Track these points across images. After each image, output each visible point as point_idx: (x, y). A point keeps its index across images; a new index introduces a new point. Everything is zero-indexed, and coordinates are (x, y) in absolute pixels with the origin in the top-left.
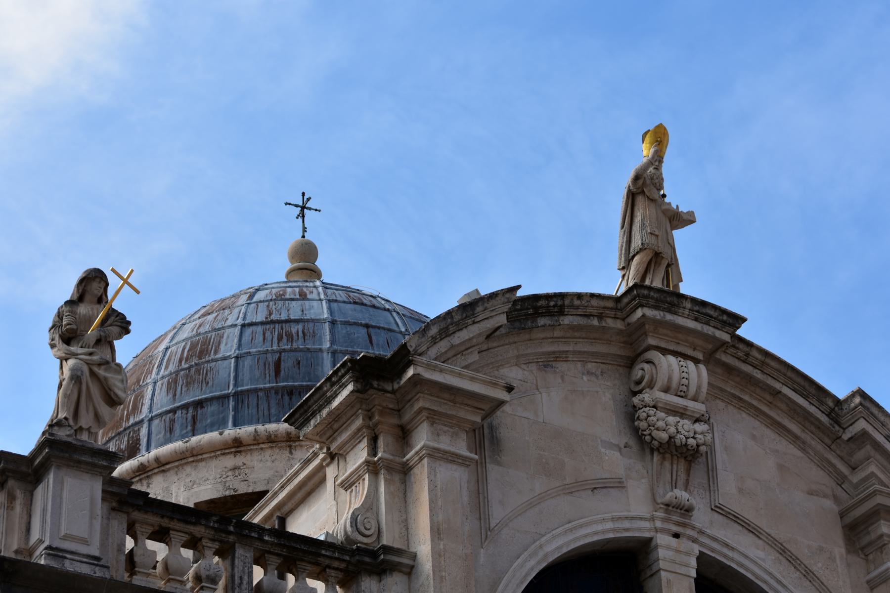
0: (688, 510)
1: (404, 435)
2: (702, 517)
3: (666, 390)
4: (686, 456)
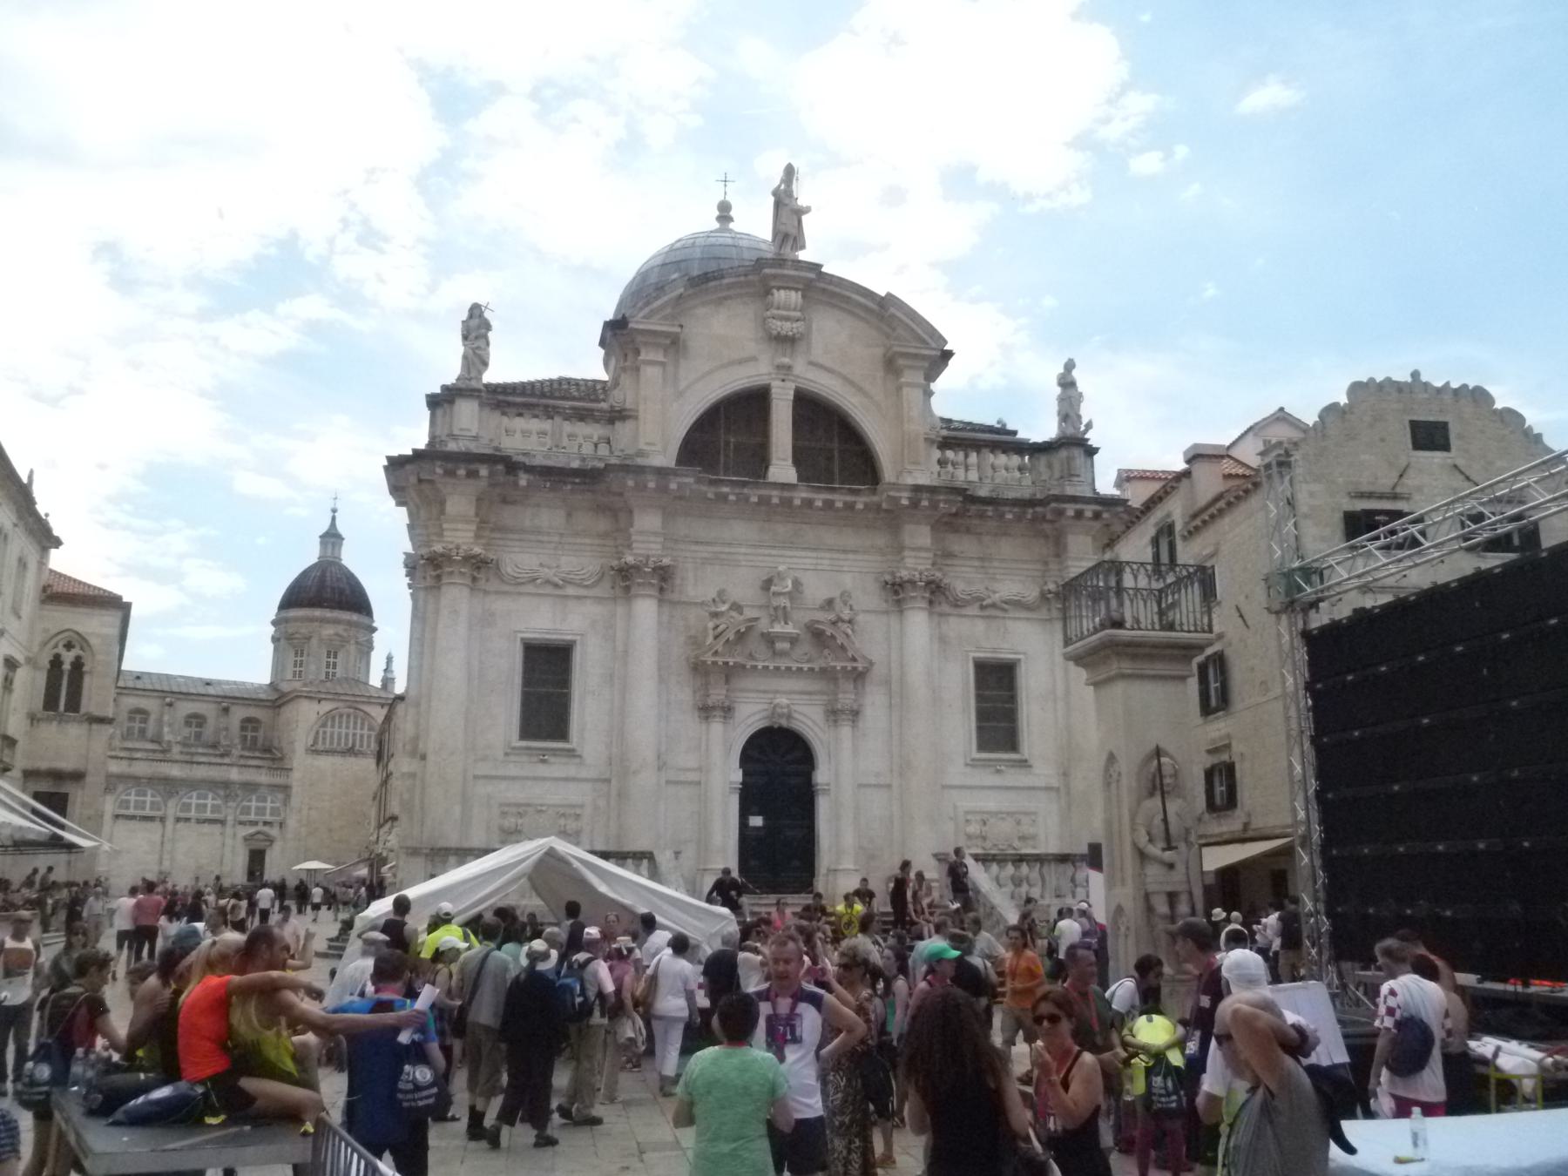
0: (789, 368)
1: (638, 352)
2: (800, 368)
4: (786, 342)
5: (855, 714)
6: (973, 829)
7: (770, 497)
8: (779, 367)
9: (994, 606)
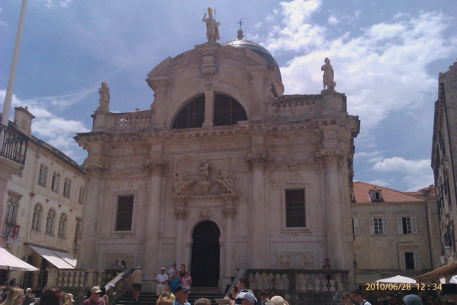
0: (210, 85)
3: (205, 63)
5: (234, 213)
6: (284, 260)
7: (200, 134)
8: (207, 85)
9: (293, 165)
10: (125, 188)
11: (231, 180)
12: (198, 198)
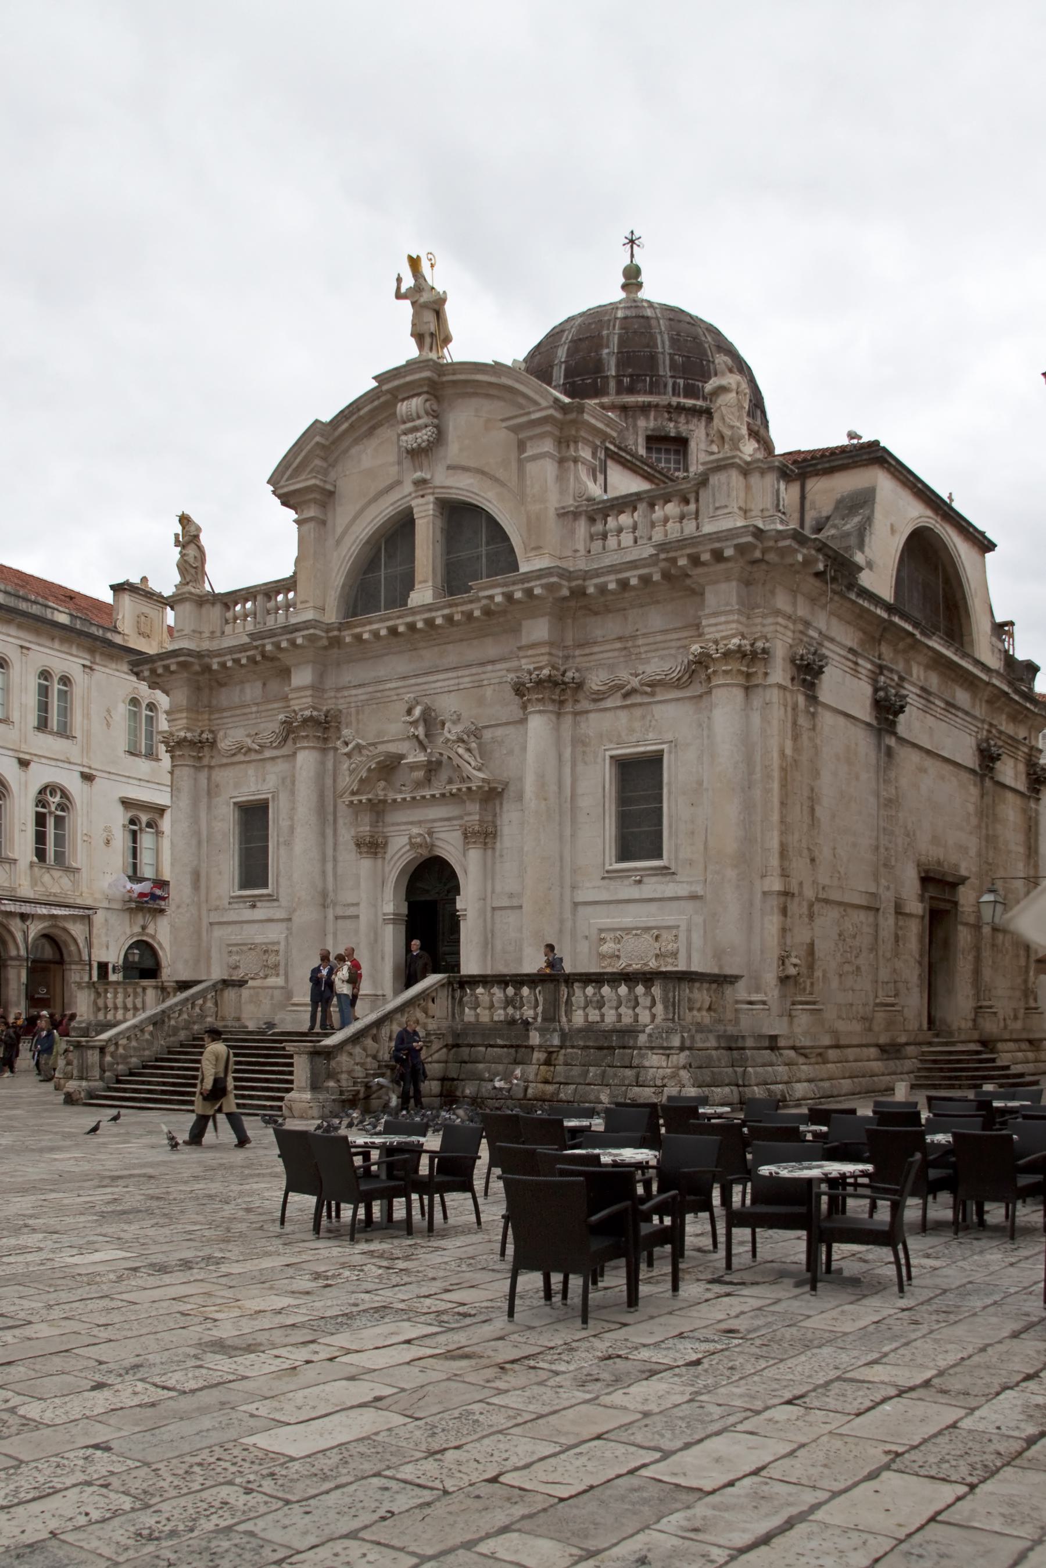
3: (404, 422)
10: (250, 784)
11: (474, 745)
12: (404, 799)
